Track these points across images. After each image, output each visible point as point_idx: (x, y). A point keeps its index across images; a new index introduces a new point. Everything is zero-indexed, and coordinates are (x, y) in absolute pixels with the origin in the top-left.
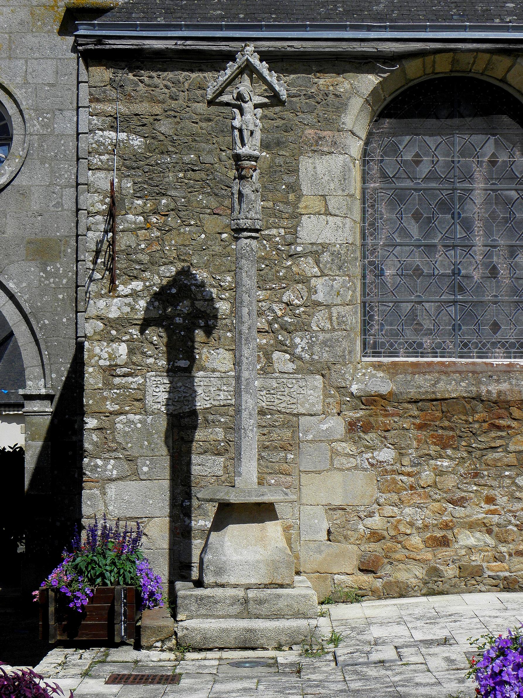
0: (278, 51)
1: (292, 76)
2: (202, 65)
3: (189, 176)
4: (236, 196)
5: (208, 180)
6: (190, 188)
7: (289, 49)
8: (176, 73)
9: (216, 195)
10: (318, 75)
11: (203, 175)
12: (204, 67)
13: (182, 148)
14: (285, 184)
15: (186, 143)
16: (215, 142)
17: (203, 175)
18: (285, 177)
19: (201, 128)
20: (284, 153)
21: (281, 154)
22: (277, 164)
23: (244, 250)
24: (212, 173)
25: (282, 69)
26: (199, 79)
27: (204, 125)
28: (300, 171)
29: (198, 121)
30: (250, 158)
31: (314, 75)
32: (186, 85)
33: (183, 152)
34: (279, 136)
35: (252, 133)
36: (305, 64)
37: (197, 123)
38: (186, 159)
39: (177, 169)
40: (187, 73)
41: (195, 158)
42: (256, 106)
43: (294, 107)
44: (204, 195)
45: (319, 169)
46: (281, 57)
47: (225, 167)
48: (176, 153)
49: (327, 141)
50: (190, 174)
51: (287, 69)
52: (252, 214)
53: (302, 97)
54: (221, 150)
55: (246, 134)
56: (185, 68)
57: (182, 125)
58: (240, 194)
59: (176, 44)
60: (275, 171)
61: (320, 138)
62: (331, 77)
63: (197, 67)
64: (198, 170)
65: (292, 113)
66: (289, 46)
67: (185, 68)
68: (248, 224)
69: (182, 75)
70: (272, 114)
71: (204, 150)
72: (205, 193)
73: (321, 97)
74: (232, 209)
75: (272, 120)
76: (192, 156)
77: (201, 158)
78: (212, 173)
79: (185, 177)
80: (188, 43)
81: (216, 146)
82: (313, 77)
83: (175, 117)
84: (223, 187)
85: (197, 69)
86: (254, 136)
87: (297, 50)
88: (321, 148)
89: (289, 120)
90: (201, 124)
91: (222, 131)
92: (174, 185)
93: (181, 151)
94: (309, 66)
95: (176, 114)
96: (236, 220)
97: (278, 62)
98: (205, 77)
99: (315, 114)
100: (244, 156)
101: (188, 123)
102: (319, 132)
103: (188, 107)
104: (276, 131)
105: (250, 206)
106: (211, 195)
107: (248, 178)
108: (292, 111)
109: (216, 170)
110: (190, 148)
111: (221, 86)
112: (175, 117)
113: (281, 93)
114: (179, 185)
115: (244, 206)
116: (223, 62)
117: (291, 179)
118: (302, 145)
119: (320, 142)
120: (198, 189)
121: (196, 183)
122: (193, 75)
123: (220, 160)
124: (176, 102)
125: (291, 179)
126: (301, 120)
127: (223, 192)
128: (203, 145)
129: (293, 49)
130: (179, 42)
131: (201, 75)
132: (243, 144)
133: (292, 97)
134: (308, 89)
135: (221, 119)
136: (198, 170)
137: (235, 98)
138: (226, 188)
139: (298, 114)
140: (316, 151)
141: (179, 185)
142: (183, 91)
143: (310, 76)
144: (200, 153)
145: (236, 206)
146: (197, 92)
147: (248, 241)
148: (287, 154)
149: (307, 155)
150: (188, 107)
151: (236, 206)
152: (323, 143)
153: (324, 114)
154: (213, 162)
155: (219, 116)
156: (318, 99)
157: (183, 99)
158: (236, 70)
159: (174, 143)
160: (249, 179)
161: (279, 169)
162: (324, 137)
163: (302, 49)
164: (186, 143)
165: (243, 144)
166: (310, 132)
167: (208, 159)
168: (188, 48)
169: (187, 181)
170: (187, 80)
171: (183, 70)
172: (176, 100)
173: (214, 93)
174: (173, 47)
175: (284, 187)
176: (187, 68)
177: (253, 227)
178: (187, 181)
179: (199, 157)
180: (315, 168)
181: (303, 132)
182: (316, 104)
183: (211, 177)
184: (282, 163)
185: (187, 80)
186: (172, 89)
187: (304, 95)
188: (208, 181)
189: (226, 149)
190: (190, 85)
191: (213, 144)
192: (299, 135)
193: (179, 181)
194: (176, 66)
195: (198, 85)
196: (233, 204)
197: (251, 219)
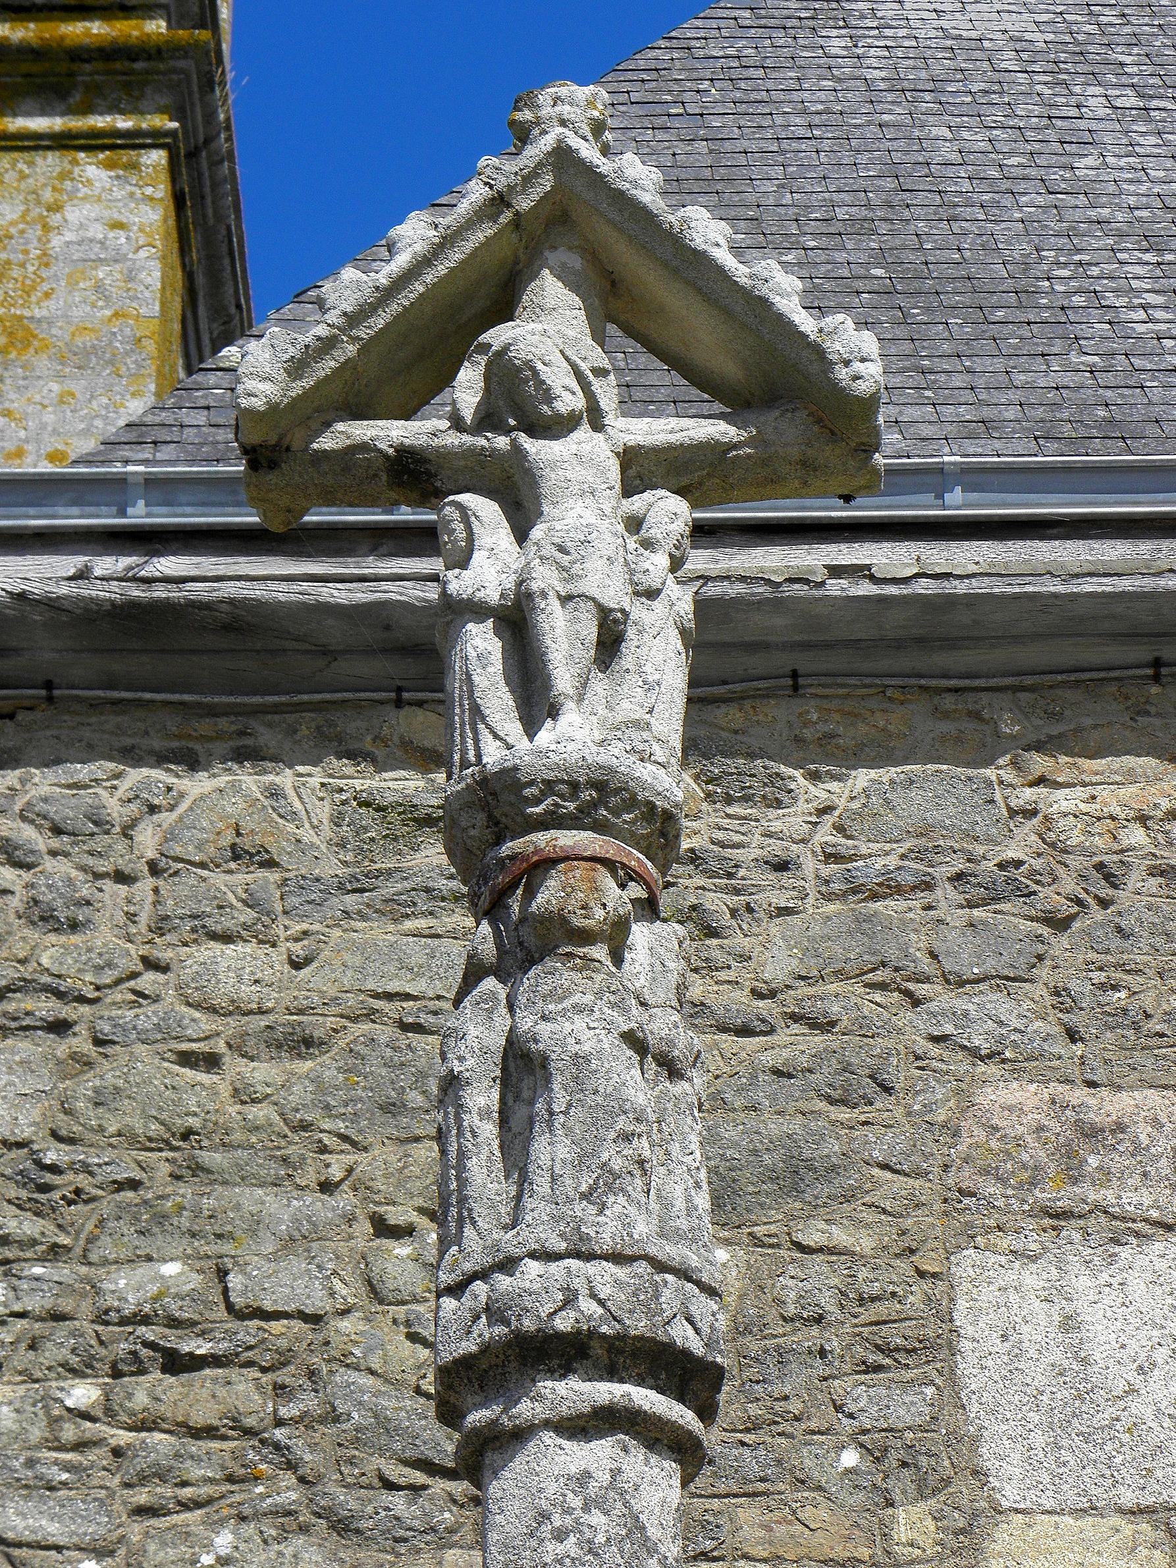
0: (760, 604)
1: (862, 777)
2: (255, 724)
3: (141, 1399)
4: (482, 1097)
5: (279, 1423)
6: (143, 1479)
7: (836, 587)
8: (83, 771)
9: (343, 1526)
10: (1039, 763)
11: (244, 1393)
12: (266, 737)
13: (101, 1223)
14: (859, 1437)
15: (134, 1185)
16: (336, 1173)
17: (244, 1393)
18: (864, 1397)
19: (244, 1095)
20: (840, 1236)
21: (813, 1238)
22: (791, 1310)
23: (560, 1535)
24: (312, 1374)
25: (798, 740)
26: (234, 807)
27: (262, 1072)
28: (965, 1345)
29: (221, 1046)
30: (597, 797)
31: (1015, 764)
32: (147, 840)
33: (106, 1248)
34: (795, 1125)
35: (610, 640)
36: (948, 702)
37: (211, 1062)
38: (127, 1287)
39: (52, 1353)
40: (156, 774)
41: (195, 1281)
42: (639, 470)
43: (892, 954)
44: (249, 1529)
45: (1102, 1333)
46: (785, 661)
47: (413, 1337)
48: (55, 1252)
49: (1137, 1149)
50: (146, 1391)
51: (832, 736)
52: (621, 1220)
53: (946, 894)
54: (383, 1229)
55: (564, 638)
56: (145, 743)
57: (108, 1075)
58: (522, 1067)
59: (82, 575)
60: (782, 1356)
61: (1091, 1133)
62: (1131, 777)
63: (220, 736)
64: (214, 1361)
65: (882, 986)
66: (836, 571)
67: (145, 743)
68: (599, 1296)
69: (115, 786)
70: (742, 996)
71: (256, 1224)
72: (257, 1516)
73: (1070, 885)
74: (448, 1209)
75: (745, 1031)
76: (171, 1269)
77: (235, 1281)
78: (312, 1374)
79: (109, 1411)
80: (169, 565)
81: (345, 1200)
82: (1008, 775)
83: (60, 1027)
84: (396, 1472)
85: (221, 747)
86: (628, 658)
87: (892, 590)
88: (1108, 1196)
89: (865, 1030)
90: (234, 1065)
91: (391, 1108)
92: (30, 1463)
93: (92, 1239)
94: (976, 716)
95: (66, 1011)
96: (482, 1275)
97: (767, 695)
98: (274, 793)
99: (1039, 991)
100: (549, 786)
101: (148, 1067)
102: (1079, 1095)
103: (151, 964)
104: (773, 1098)
105: (614, 1156)
106: (304, 1529)
107: (586, 937)
108: (880, 976)
109: (345, 1361)
110: (161, 1218)
111: (353, 319)
112: (60, 1027)
113: (835, 347)
114: (67, 1467)
115: (550, 1151)
116: (399, 703)
117: (903, 1404)
118: (966, 1177)
119: (1093, 1161)
120: (205, 1491)
121: (196, 1447)
122: (197, 785)
123: (375, 1292)
124: (75, 939)
125: (903, 1404)
126: (949, 1029)
127: (398, 1502)
128: (250, 1198)
129: (865, 589)
130: (105, 565)
131: (249, 780)
132: (535, 701)
133: (875, 897)
134: (980, 850)
135: (385, 1033)
136: (214, 1361)
137: (468, 414)
138: (419, 1477)
139: (922, 990)
140: (1065, 1215)
141: (67, 1467)
142: (122, 877)
143: (990, 773)
144: (227, 1248)
145: (485, 1176)
146: (218, 879)
147: (599, 1455)
148: (866, 1243)
149: (1006, 1242)
150: (151, 964)
151: (485, 1176)
152: (1117, 1162)
153: (1102, 987)
154: (317, 1302)
155: (371, 1015)
156: (1051, 898)
157: (121, 918)
158: (469, 224)
159: (45, 1188)
160: (600, 952)
161: (811, 1336)
162: (1120, 1127)
163: (924, 587)
164: (134, 1185)
165: (535, 701)
166: (1014, 1100)
167: (289, 1284)
168: (160, 592)
169: (124, 1437)
170: (153, 809)
171: (132, 756)
172: (74, 926)
173: (296, 368)
174: (64, 589)
175: (850, 1458)
176: (157, 744)
177: (639, 1325)
178: (124, 1437)
179: (222, 1274)
180: (1069, 1323)
181: (966, 1103)
182: (1045, 931)
183: (308, 1402)
184: (827, 1301)
185: (153, 809)
186: (49, 864)
187: (959, 877)
188: (279, 1434)
189: (415, 1217)
190: (170, 836)
191: (327, 1187)
192: (941, 1116)
193: (69, 1432)
194: (87, 733)
195: (228, 838)
196: (452, 1166)
197: (617, 1258)
